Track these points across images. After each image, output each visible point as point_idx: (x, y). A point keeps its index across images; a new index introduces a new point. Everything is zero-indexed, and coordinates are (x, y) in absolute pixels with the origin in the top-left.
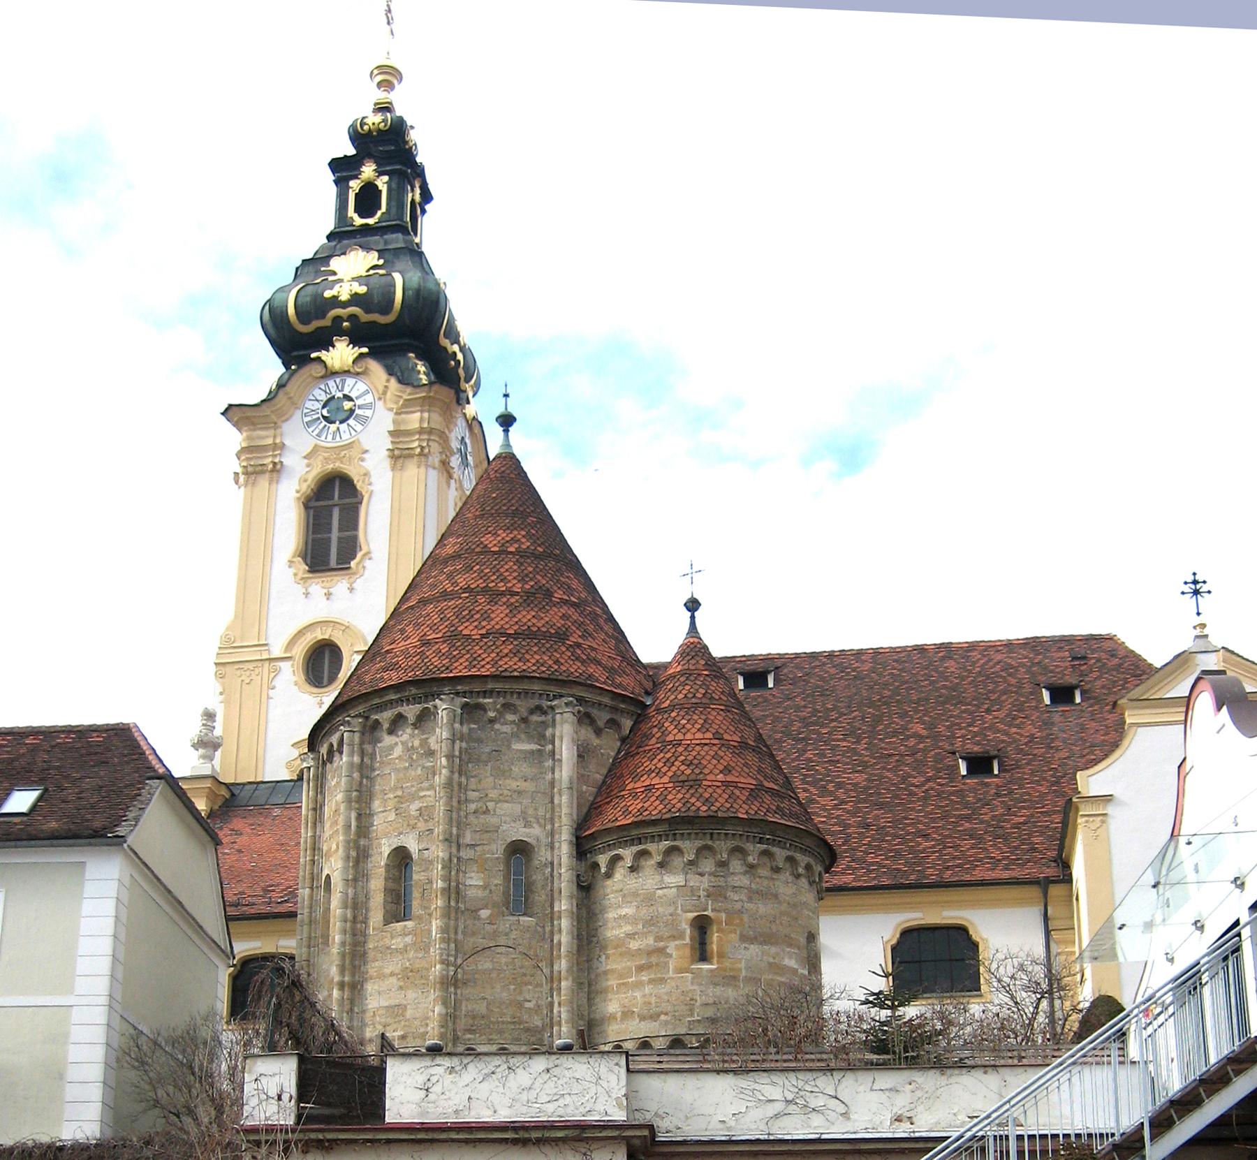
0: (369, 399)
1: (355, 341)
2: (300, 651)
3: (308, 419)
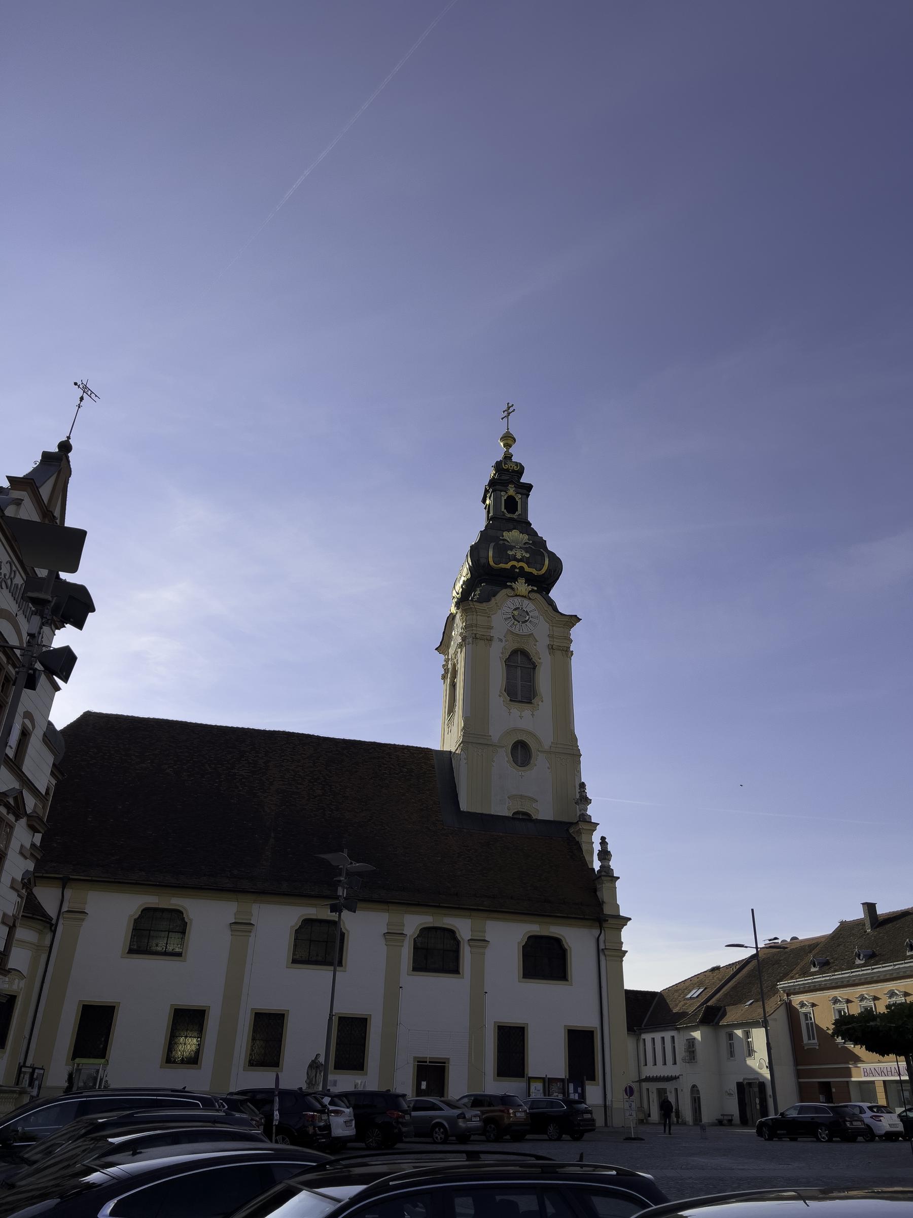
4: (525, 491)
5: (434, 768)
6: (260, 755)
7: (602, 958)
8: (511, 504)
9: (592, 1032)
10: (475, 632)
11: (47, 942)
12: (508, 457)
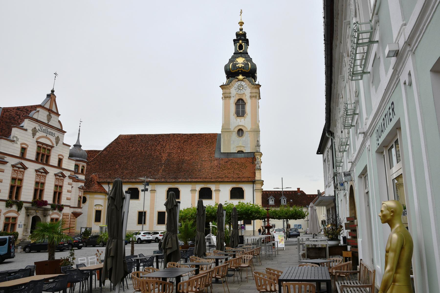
0: (246, 86)
1: (243, 76)
2: (236, 130)
12: (241, 30)
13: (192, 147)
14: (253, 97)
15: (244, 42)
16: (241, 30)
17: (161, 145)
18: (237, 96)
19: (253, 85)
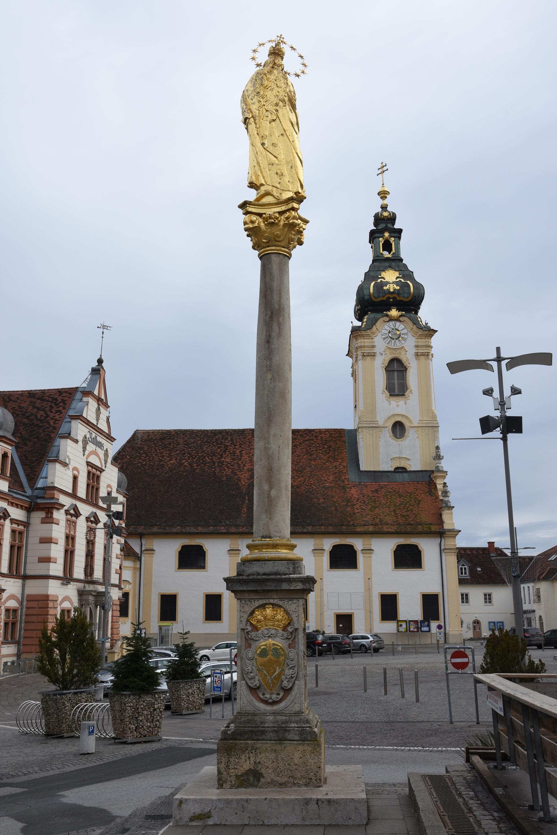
1: (399, 310)
2: (390, 424)
3: (383, 337)
4: (397, 235)
5: (345, 443)
6: (237, 447)
7: (443, 555)
8: (387, 246)
9: (437, 595)
10: (363, 351)
11: (138, 566)
12: (384, 208)
13: (297, 458)
14: (423, 354)
15: (393, 235)
16: (384, 208)
17: (231, 453)
18: (388, 352)
19: (421, 331)
